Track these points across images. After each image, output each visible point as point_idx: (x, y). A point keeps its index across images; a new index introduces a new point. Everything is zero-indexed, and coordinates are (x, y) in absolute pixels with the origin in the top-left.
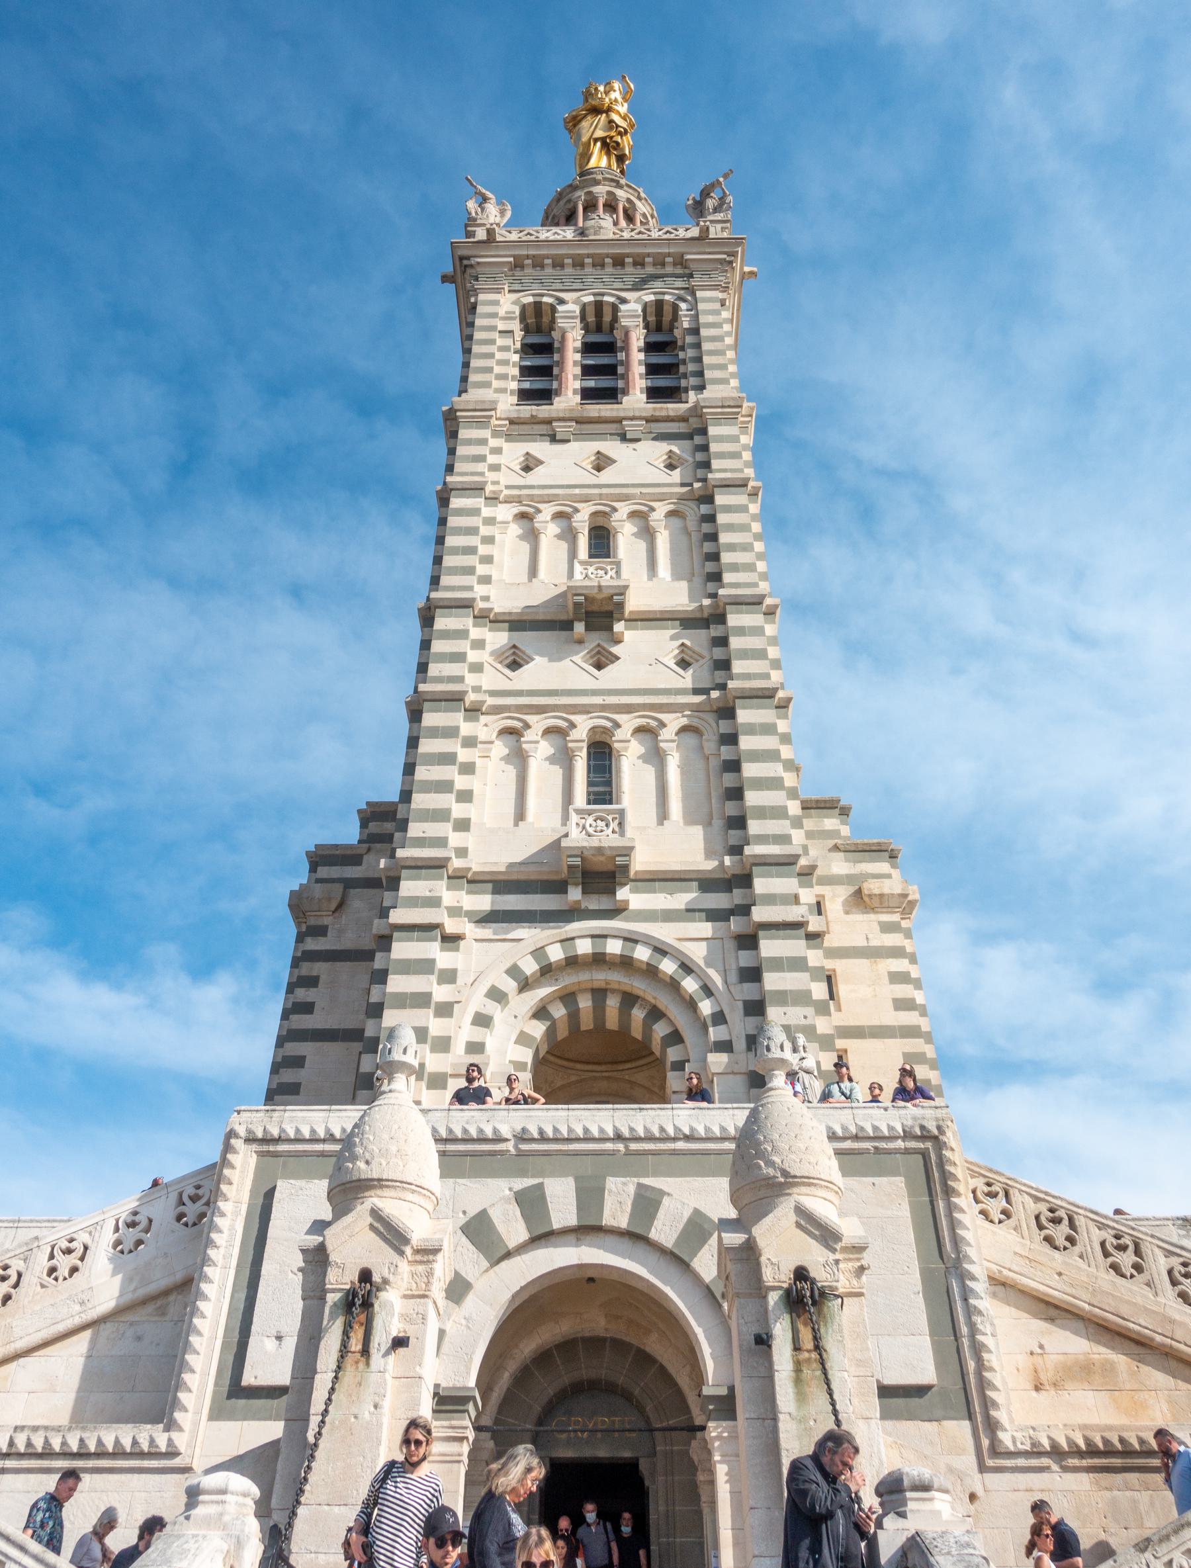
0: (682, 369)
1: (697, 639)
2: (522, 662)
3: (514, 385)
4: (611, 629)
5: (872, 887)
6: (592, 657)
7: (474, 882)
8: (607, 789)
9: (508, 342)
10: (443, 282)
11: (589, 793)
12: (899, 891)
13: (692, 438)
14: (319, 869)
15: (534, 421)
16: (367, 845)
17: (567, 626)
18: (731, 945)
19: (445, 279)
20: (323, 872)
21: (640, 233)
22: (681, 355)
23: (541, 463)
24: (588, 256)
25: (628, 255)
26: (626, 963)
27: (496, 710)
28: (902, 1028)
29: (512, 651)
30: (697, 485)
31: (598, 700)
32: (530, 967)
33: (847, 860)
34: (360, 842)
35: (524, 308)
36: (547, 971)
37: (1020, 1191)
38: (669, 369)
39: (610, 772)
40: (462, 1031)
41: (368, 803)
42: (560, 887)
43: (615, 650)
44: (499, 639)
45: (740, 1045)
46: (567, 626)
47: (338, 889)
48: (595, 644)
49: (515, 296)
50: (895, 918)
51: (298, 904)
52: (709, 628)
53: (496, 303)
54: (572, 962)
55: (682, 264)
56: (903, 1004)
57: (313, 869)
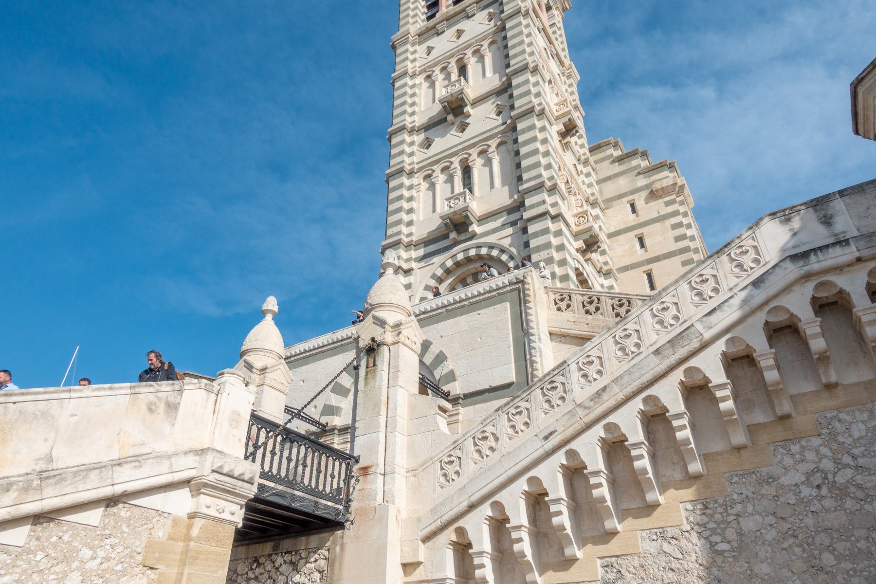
1: (501, 100)
5: (657, 186)
6: (459, 129)
7: (417, 245)
12: (672, 183)
17: (445, 120)
27: (420, 169)
28: (679, 250)
31: (460, 147)
32: (440, 272)
33: (645, 177)
37: (575, 294)
43: (467, 121)
44: (419, 138)
48: (459, 122)
54: (458, 265)
56: (678, 239)
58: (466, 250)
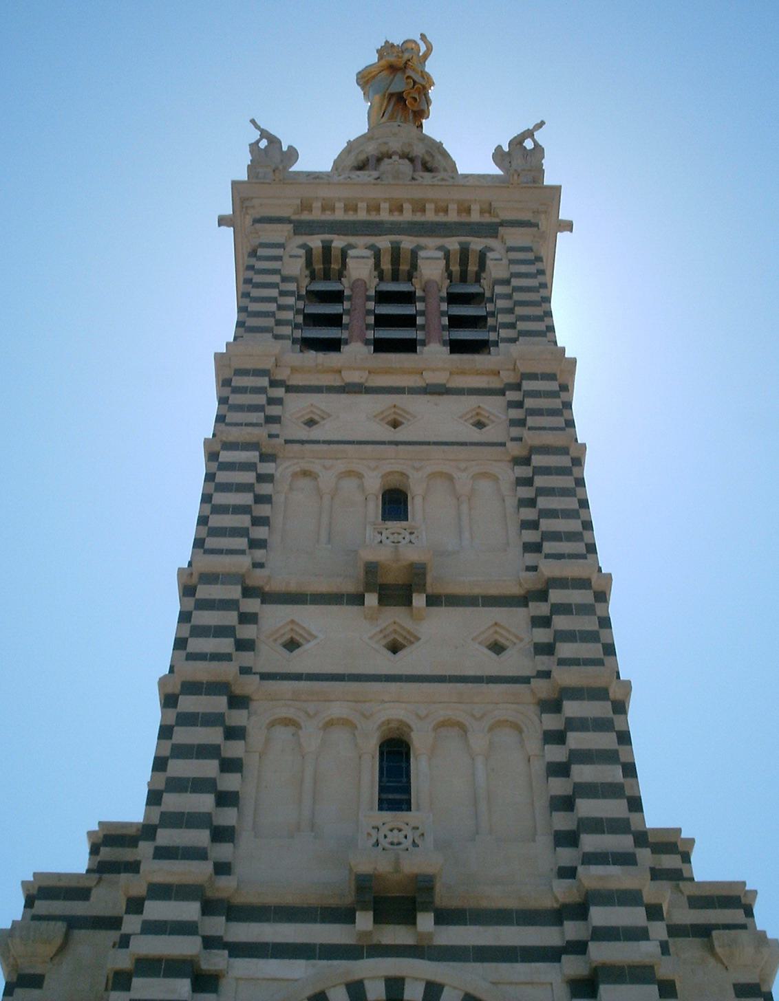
0: (490, 321)
2: (301, 641)
3: (298, 334)
4: (409, 603)
6: (385, 637)
8: (404, 797)
9: (292, 287)
10: (220, 225)
11: (381, 801)
13: (504, 395)
14: (37, 903)
16: (97, 876)
19: (222, 221)
20: (42, 907)
21: (443, 180)
22: (490, 307)
23: (329, 416)
24: (385, 200)
25: (431, 201)
29: (289, 627)
30: (509, 444)
34: (88, 871)
35: (309, 252)
39: (408, 776)
41: (100, 823)
42: (345, 916)
46: (358, 599)
47: (61, 926)
49: (301, 240)
52: (526, 606)
55: (490, 213)
57: (29, 902)
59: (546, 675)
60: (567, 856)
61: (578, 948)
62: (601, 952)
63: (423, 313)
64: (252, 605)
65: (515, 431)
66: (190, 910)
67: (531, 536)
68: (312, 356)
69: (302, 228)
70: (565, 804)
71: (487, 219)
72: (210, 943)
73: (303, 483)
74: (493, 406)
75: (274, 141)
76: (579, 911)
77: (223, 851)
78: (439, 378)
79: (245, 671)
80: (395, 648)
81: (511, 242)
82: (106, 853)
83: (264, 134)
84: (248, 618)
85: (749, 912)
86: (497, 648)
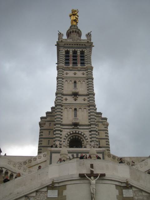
0: (85, 60)
3: (65, 62)
15: (67, 68)
18: (89, 132)
19: (55, 45)
20: (43, 120)
26: (78, 133)
35: (66, 51)
36: (71, 134)
38: (83, 60)
40: (63, 140)
45: (89, 142)
49: (64, 49)
50: (106, 126)
51: (40, 124)
53: (62, 50)
54: (73, 133)
58: (76, 131)
59: (88, 104)
60: (90, 121)
61: (90, 128)
62: (92, 129)
63: (78, 59)
64: (62, 96)
65: (87, 76)
66: (59, 126)
67: (88, 89)
68: (66, 67)
69: (65, 47)
70: (89, 116)
71: (85, 46)
72: (61, 128)
73: (66, 82)
74: (85, 72)
75: (61, 34)
76: (90, 125)
77: (61, 120)
78: (79, 69)
79: (63, 103)
80: (75, 100)
81: (87, 50)
82: (48, 115)
83: (59, 33)
84: (62, 98)
85: (107, 120)
86: (84, 100)
